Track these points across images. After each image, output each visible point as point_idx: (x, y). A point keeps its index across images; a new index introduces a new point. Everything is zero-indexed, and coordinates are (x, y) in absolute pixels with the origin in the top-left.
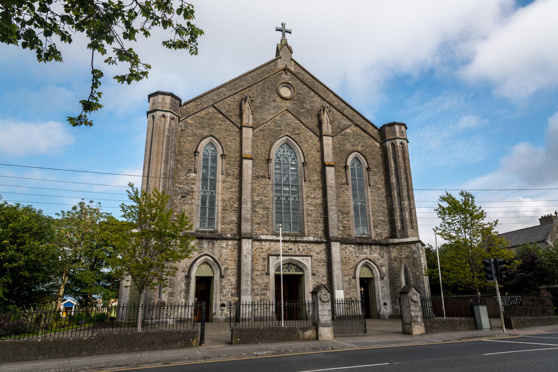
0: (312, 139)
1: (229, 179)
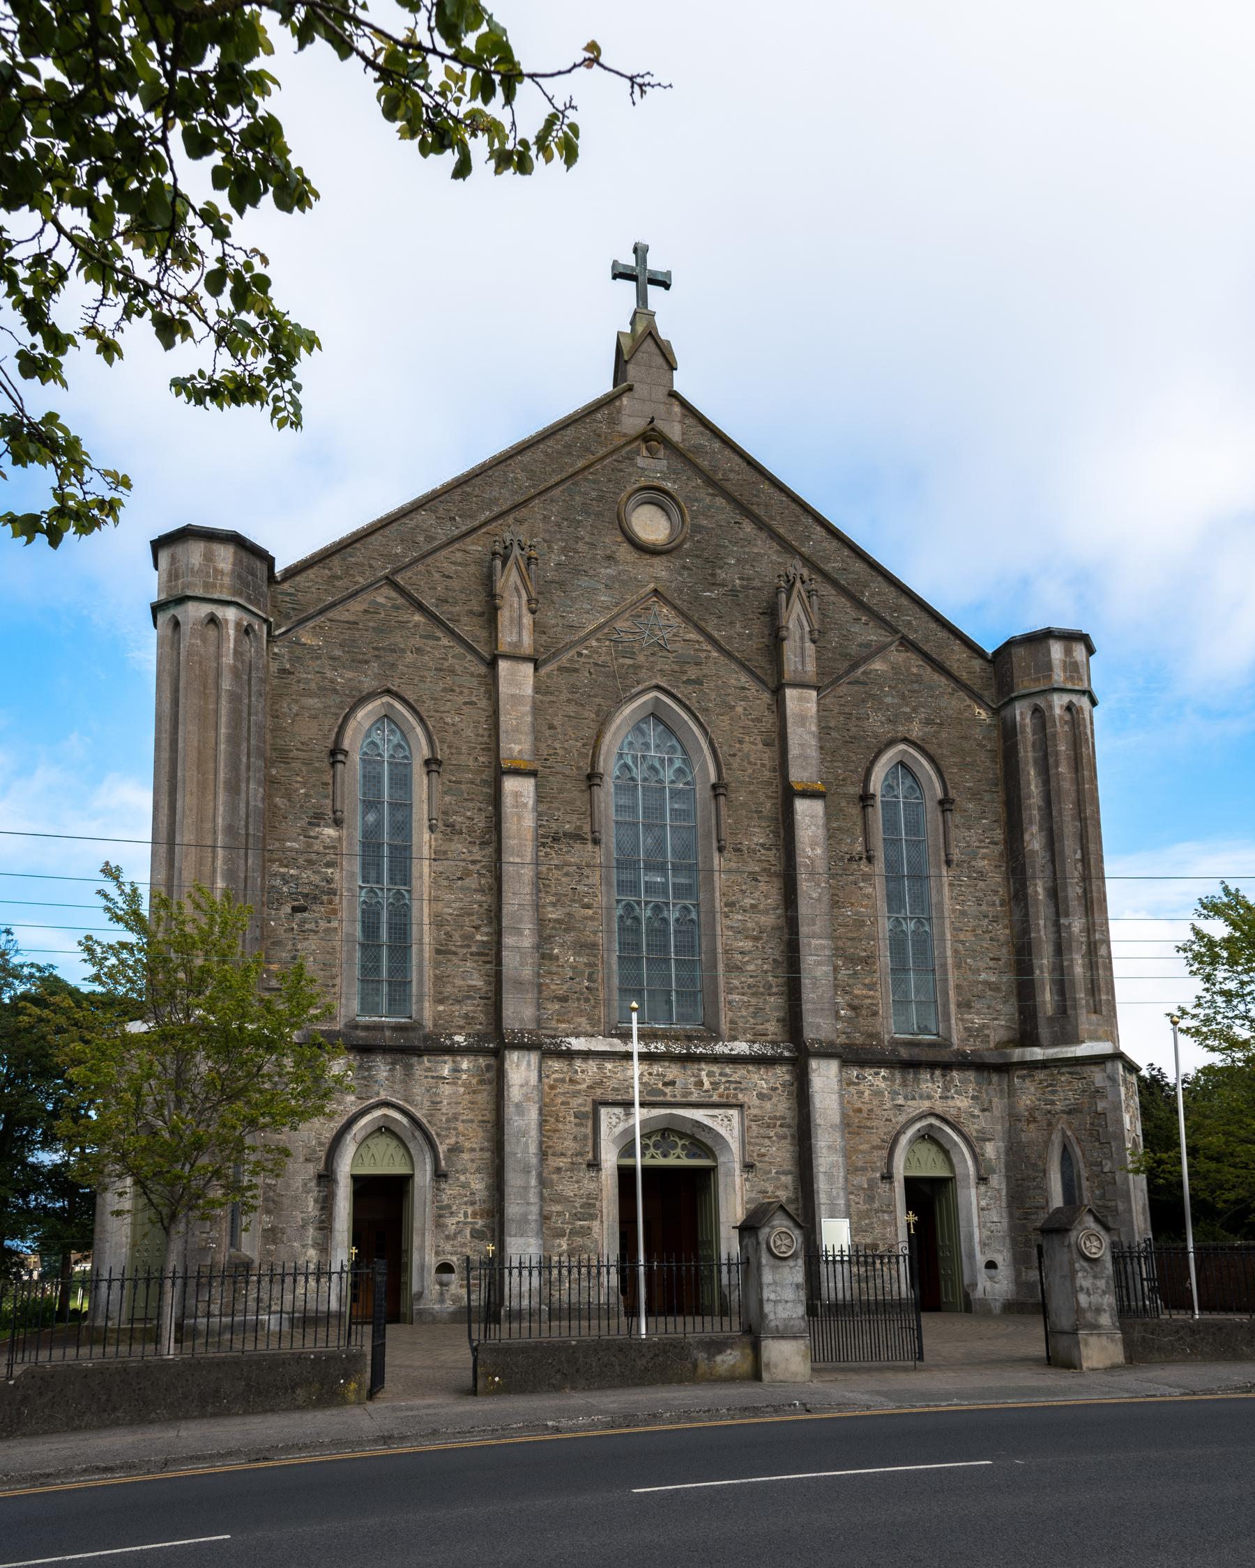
0: (745, 699)
1: (458, 846)
